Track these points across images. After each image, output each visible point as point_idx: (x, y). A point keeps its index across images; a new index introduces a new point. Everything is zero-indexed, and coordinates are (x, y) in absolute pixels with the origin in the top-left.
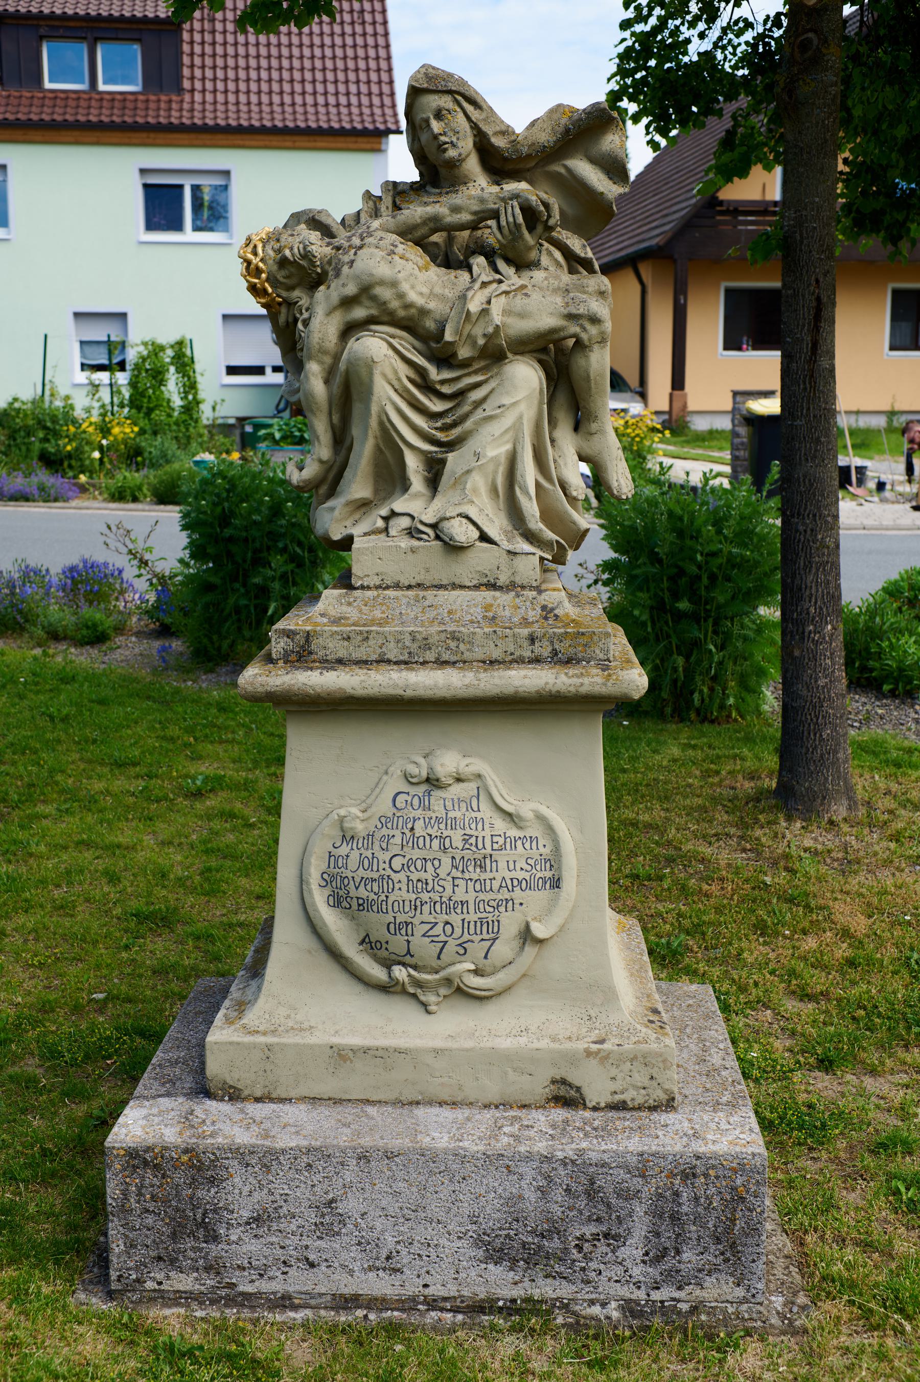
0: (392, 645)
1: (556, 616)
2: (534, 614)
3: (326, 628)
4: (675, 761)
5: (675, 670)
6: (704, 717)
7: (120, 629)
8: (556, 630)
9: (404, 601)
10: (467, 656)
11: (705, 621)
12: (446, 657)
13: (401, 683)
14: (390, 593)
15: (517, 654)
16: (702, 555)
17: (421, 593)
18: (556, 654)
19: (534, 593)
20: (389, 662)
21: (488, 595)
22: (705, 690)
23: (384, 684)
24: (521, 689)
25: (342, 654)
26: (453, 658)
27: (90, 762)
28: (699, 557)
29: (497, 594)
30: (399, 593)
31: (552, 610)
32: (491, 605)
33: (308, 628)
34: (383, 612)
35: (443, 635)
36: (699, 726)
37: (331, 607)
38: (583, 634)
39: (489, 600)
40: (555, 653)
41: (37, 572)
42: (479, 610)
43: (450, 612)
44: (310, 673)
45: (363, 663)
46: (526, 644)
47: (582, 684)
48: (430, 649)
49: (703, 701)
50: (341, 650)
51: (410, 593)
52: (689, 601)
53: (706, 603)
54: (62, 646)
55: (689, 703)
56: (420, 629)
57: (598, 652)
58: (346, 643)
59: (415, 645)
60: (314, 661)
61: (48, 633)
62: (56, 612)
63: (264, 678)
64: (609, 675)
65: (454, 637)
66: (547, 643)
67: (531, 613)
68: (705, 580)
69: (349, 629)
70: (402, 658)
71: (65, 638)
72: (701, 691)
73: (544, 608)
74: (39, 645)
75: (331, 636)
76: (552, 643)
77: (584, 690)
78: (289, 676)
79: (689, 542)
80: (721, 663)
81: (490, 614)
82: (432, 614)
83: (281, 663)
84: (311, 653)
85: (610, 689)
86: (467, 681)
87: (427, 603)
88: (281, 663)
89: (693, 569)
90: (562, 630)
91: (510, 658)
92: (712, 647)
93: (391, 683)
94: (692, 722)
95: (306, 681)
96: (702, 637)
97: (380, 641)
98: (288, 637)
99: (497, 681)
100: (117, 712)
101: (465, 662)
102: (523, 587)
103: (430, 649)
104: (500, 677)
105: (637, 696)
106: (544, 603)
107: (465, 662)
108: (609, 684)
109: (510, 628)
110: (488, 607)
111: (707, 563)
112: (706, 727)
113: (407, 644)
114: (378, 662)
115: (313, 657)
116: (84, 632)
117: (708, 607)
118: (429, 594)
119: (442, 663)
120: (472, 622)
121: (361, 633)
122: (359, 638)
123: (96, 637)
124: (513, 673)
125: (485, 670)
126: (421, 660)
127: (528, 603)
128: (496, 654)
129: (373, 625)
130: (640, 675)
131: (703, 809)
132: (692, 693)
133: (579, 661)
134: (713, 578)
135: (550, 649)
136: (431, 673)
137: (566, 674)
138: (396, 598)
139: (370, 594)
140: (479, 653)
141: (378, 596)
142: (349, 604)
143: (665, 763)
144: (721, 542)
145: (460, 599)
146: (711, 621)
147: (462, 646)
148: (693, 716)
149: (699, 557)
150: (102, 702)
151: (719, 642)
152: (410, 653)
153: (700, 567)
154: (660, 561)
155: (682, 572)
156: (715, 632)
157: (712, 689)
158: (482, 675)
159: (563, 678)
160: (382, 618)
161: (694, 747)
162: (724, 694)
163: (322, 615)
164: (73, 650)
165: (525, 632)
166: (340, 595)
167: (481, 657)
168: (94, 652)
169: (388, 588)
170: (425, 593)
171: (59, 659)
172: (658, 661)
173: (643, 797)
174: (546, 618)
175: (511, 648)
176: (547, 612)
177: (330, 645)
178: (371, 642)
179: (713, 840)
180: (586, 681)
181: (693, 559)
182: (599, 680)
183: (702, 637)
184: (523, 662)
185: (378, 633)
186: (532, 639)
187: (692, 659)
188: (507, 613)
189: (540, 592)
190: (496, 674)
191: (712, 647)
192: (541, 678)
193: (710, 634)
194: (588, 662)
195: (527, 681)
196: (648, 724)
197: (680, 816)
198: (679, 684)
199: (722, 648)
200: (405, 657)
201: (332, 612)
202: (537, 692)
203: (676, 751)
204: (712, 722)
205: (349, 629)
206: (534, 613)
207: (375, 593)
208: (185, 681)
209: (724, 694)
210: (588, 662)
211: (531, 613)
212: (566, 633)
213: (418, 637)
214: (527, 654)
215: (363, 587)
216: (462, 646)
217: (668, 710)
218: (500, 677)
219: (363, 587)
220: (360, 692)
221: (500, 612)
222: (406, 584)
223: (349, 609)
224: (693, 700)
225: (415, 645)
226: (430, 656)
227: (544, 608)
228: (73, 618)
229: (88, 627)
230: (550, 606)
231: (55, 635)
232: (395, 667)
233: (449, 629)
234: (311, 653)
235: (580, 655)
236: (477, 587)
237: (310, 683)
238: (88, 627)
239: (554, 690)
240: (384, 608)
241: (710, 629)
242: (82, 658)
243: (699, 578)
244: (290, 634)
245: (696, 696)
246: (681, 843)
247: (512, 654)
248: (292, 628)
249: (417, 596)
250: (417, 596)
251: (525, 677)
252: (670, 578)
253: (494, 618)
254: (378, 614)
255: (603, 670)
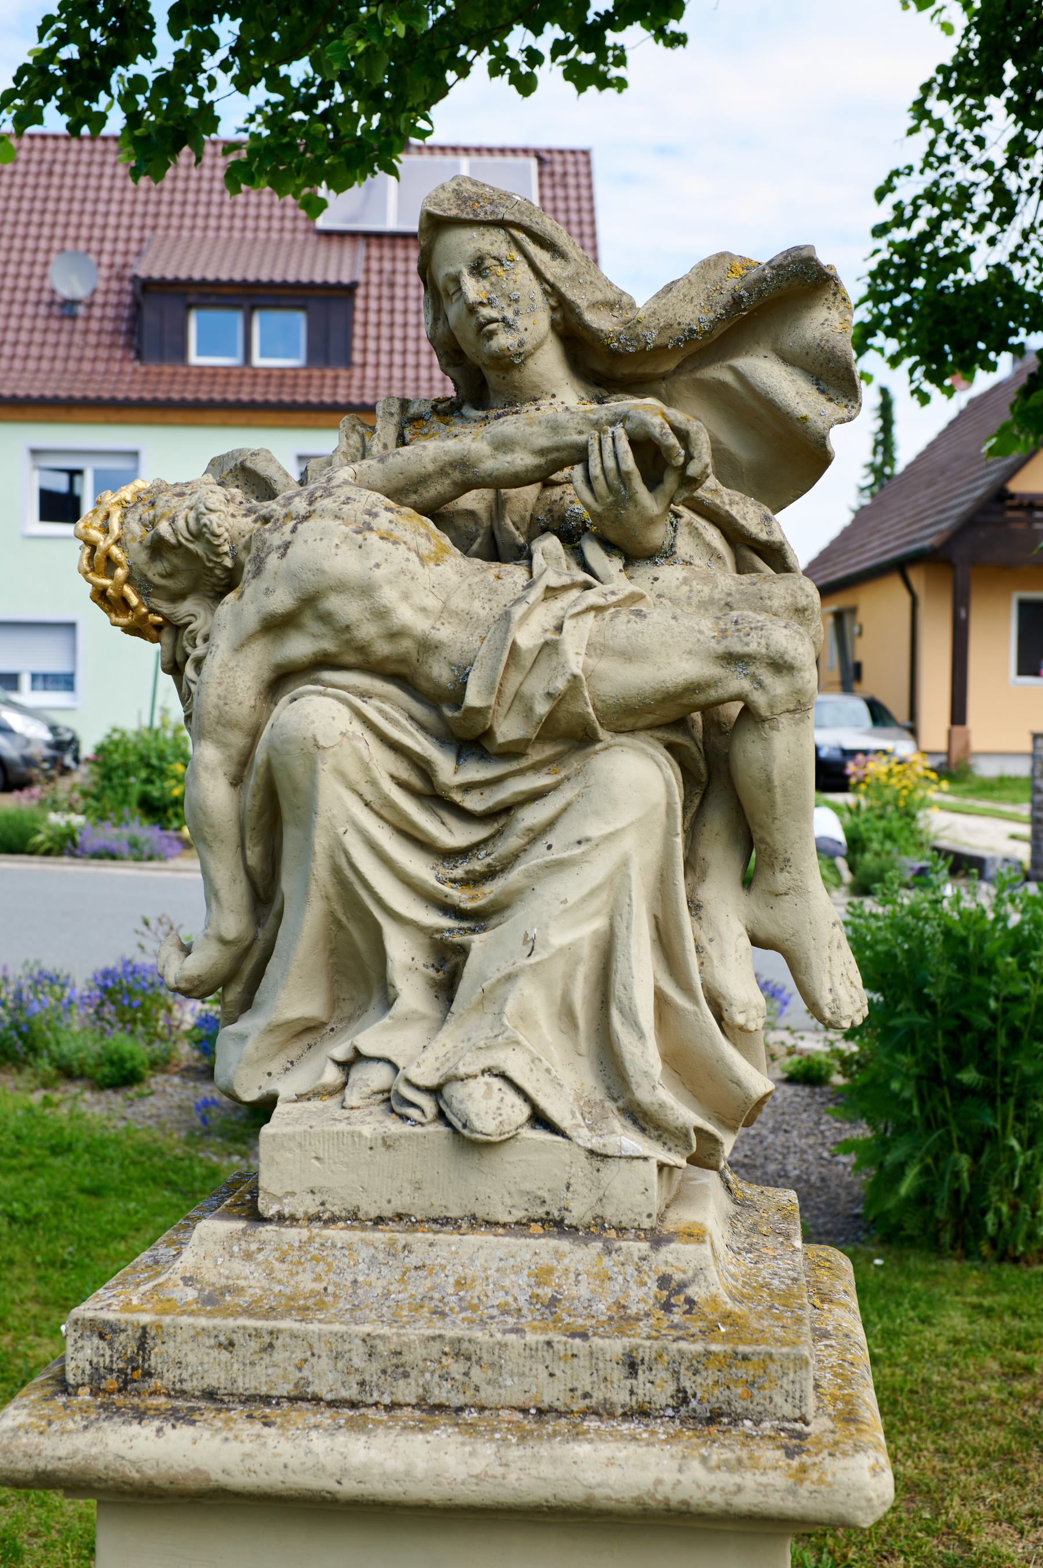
0: (324, 1363)
1: (690, 1301)
2: (641, 1296)
3: (185, 1320)
4: (956, 1342)
5: (957, 1175)
6: (1005, 1256)
7: (160, 1064)
8: (683, 1345)
9: (365, 1253)
10: (488, 1395)
11: (1004, 1100)
12: (441, 1394)
13: (331, 1462)
14: (336, 1234)
15: (598, 1395)
16: (997, 998)
17: (402, 1238)
18: (685, 1401)
19: (644, 1246)
20: (316, 1399)
21: (544, 1247)
22: (1005, 1209)
23: (293, 1463)
24: (600, 1493)
25: (215, 1378)
26: (457, 1400)
27: (45, 1302)
28: (993, 1004)
29: (564, 1245)
30: (356, 1236)
31: (682, 1286)
32: (550, 1271)
33: (145, 1319)
34: (318, 1279)
35: (435, 1348)
36: (995, 1268)
37: (209, 1263)
38: (745, 1358)
39: (546, 1259)
40: (682, 1397)
41: (53, 980)
42: (523, 1280)
43: (460, 1284)
44: (135, 1428)
45: (258, 1402)
46: (618, 1374)
47: (739, 1489)
48: (406, 1375)
49: (1000, 1225)
50: (212, 1369)
51: (379, 1236)
52: (979, 1069)
53: (1005, 1073)
54: (74, 1089)
55: (979, 1227)
56: (385, 1330)
57: (779, 1399)
58: (225, 1356)
59: (375, 1367)
60: (154, 1393)
61: (59, 1068)
62: (77, 1036)
63: (34, 1438)
64: (803, 1469)
65: (459, 1351)
66: (666, 1375)
67: (636, 1293)
68: (1002, 1040)
69: (231, 1323)
70: (344, 1394)
71: (82, 1076)
72: (998, 1211)
73: (664, 1281)
74: (45, 1086)
75: (194, 1338)
76: (676, 1375)
77: (744, 1502)
78: (90, 1435)
79: (976, 980)
80: (1028, 1167)
81: (546, 1292)
82: (419, 1286)
83: (84, 1395)
84: (148, 1374)
85: (802, 1502)
86: (478, 1466)
87: (413, 1260)
88: (84, 1395)
89: (983, 1021)
90: (698, 1347)
91: (583, 1404)
92: (1014, 1143)
93: (310, 1461)
94: (984, 1259)
95: (123, 1450)
96: (998, 1126)
97: (299, 1355)
98: (102, 1337)
99: (546, 1470)
100: (114, 1208)
101: (482, 1409)
102: (621, 1230)
103: (406, 1375)
104: (554, 1461)
105: (866, 1521)
106: (663, 1269)
107: (482, 1409)
108: (803, 1491)
109: (584, 1336)
110: (542, 1276)
111: (1005, 1011)
112: (1007, 1270)
113: (357, 1362)
114: (292, 1399)
115: (154, 1383)
116: (106, 1070)
117: (1007, 1080)
118: (420, 1238)
119: (433, 1410)
120: (505, 1311)
121: (257, 1334)
122: (254, 1345)
123: (121, 1077)
124: (582, 1449)
125: (523, 1437)
126: (387, 1400)
127: (630, 1269)
128: (552, 1394)
129: (287, 1313)
130: (875, 1471)
131: (1006, 1454)
132: (984, 1213)
133: (736, 1420)
134: (1014, 1035)
135: (671, 1388)
136: (401, 1441)
137: (704, 1460)
138: (349, 1247)
139: (293, 1234)
140: (512, 1390)
141: (311, 1240)
142: (248, 1256)
143: (941, 1347)
144: (1026, 981)
145: (482, 1254)
146: (1011, 1101)
147: (476, 1373)
148: (985, 1248)
149: (993, 1004)
150: (95, 1192)
151: (1025, 1133)
152: (362, 1384)
153: (993, 1018)
154: (932, 1007)
155: (965, 1025)
156: (1018, 1118)
157: (1014, 1208)
158: (514, 1453)
159: (696, 1471)
160: (313, 1294)
161: (989, 1313)
162: (1034, 1216)
163: (188, 1281)
164: (88, 1096)
165: (616, 1346)
166: (231, 1236)
167: (519, 1399)
168: (116, 1099)
169: (333, 1220)
170: (409, 1238)
171: (64, 1111)
172: (929, 1160)
173: (905, 1420)
174: (667, 1307)
175: (585, 1383)
176: (671, 1290)
177: (191, 1358)
178: (279, 1356)
179: (1027, 1524)
180: (749, 1479)
181: (984, 1007)
182: (778, 1480)
183: (998, 1126)
184: (612, 1415)
185: (294, 1336)
186: (632, 1365)
187: (984, 1159)
188: (583, 1291)
189: (658, 1240)
190: (544, 1450)
191: (1014, 1143)
192: (645, 1467)
193: (1011, 1122)
194: (757, 1423)
195: (614, 1475)
196: (914, 1262)
197: (968, 1470)
198: (963, 1198)
199: (1029, 1143)
200: (352, 1392)
201: (210, 1275)
202: (637, 1500)
203: (957, 1321)
204: (1016, 1260)
205: (231, 1323)
206: (641, 1292)
207: (305, 1233)
208: (230, 1154)
209: (1034, 1216)
210: (757, 1423)
211: (636, 1293)
212: (708, 1353)
213: (381, 1347)
214: (620, 1397)
215: (281, 1219)
216: (476, 1373)
217: (946, 1238)
218: (554, 1461)
219: (281, 1219)
220: (240, 1480)
221: (569, 1289)
222: (373, 1214)
223: (247, 1268)
224: (985, 1224)
225: (375, 1367)
226: (407, 1391)
227: (664, 1281)
228: (97, 1048)
229: (112, 1063)
230: (678, 1277)
231: (67, 1073)
232: (325, 1417)
233: (450, 1333)
234: (148, 1374)
235: (739, 1406)
236: (522, 1227)
237: (131, 1455)
238: (112, 1063)
239: (675, 1498)
240: (321, 1268)
241: (1011, 1114)
242: (94, 1110)
243: (993, 1034)
244: (104, 1331)
245: (990, 1219)
246: (970, 1531)
247: (586, 1395)
248: (110, 1316)
249: (393, 1243)
250: (393, 1243)
251: (610, 1462)
252: (950, 1034)
253: (554, 1301)
254: (306, 1282)
255: (790, 1454)
